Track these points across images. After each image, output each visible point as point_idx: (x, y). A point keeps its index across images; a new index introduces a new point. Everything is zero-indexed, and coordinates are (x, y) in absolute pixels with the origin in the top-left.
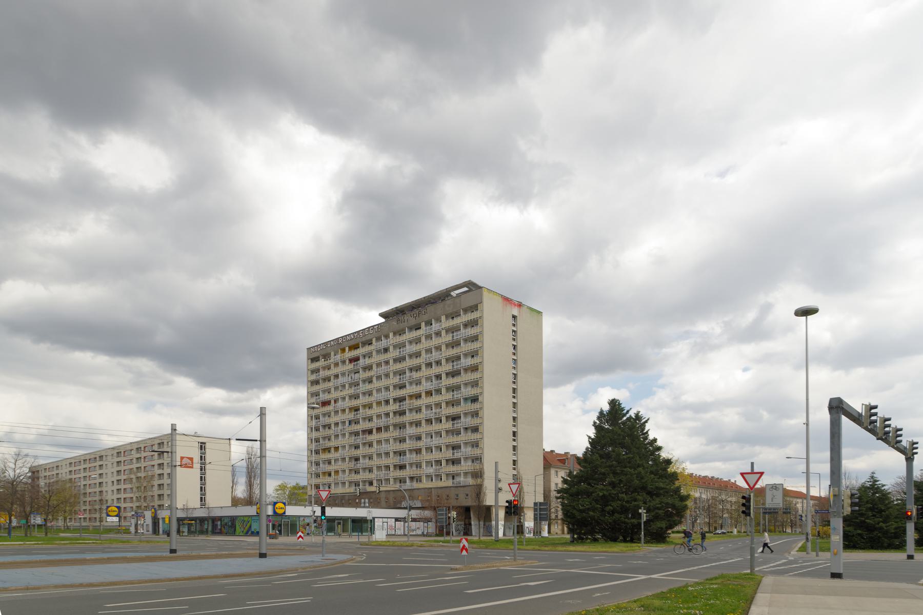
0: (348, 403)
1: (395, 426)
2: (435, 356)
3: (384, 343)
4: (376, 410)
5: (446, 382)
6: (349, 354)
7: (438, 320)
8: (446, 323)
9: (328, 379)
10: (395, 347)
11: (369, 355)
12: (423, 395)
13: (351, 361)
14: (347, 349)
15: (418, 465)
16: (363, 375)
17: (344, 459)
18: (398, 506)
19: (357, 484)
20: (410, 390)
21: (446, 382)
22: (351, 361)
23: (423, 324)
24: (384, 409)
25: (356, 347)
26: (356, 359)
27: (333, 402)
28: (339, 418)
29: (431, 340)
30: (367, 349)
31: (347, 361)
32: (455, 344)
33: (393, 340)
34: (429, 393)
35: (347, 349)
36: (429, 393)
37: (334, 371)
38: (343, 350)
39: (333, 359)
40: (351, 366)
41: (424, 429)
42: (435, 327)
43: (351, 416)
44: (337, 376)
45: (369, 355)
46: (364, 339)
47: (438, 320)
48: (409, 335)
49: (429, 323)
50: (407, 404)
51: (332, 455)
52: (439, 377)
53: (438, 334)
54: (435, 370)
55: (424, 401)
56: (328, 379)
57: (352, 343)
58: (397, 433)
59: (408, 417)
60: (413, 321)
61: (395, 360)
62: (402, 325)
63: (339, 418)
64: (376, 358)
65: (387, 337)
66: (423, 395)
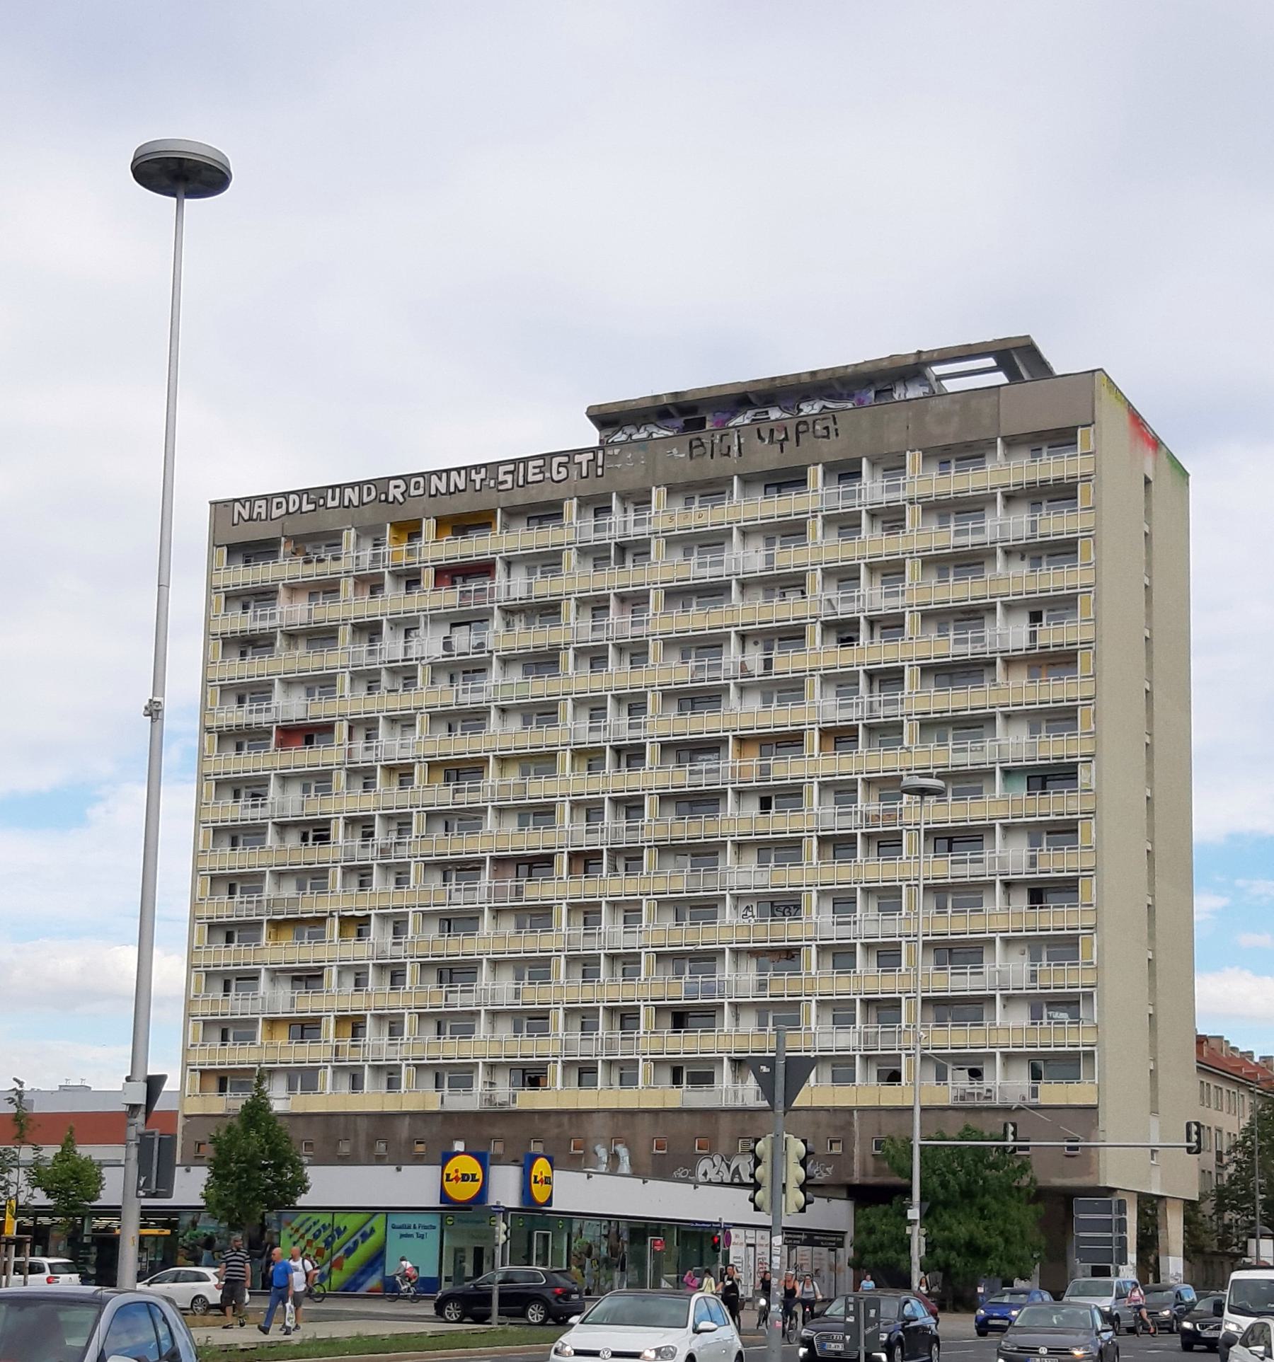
0: (424, 743)
1: (668, 850)
2: (871, 597)
4: (568, 781)
5: (919, 699)
6: (435, 549)
7: (893, 465)
9: (322, 636)
10: (672, 542)
11: (549, 561)
12: (813, 740)
13: (448, 574)
14: (429, 526)
15: (785, 1013)
16: (497, 637)
17: (396, 974)
19: (461, 1075)
20: (744, 713)
21: (919, 699)
22: (448, 574)
23: (816, 474)
24: (613, 780)
26: (484, 569)
27: (342, 730)
28: (383, 797)
29: (863, 538)
30: (523, 538)
31: (428, 576)
32: (969, 561)
33: (665, 514)
34: (840, 737)
35: (429, 526)
36: (840, 737)
37: (351, 606)
38: (410, 530)
39: (355, 554)
40: (449, 598)
41: (813, 871)
42: (872, 489)
43: (432, 793)
44: (369, 630)
45: (549, 561)
46: (520, 498)
47: (893, 465)
48: (745, 507)
49: (846, 472)
50: (733, 767)
51: (332, 950)
52: (888, 678)
53: (891, 518)
54: (871, 651)
55: (812, 764)
56: (322, 636)
57: (461, 505)
58: (678, 879)
59: (738, 819)
60: (767, 457)
61: (678, 595)
62: (712, 467)
63: (383, 797)
64: (576, 578)
65: (640, 500)
66: (813, 740)
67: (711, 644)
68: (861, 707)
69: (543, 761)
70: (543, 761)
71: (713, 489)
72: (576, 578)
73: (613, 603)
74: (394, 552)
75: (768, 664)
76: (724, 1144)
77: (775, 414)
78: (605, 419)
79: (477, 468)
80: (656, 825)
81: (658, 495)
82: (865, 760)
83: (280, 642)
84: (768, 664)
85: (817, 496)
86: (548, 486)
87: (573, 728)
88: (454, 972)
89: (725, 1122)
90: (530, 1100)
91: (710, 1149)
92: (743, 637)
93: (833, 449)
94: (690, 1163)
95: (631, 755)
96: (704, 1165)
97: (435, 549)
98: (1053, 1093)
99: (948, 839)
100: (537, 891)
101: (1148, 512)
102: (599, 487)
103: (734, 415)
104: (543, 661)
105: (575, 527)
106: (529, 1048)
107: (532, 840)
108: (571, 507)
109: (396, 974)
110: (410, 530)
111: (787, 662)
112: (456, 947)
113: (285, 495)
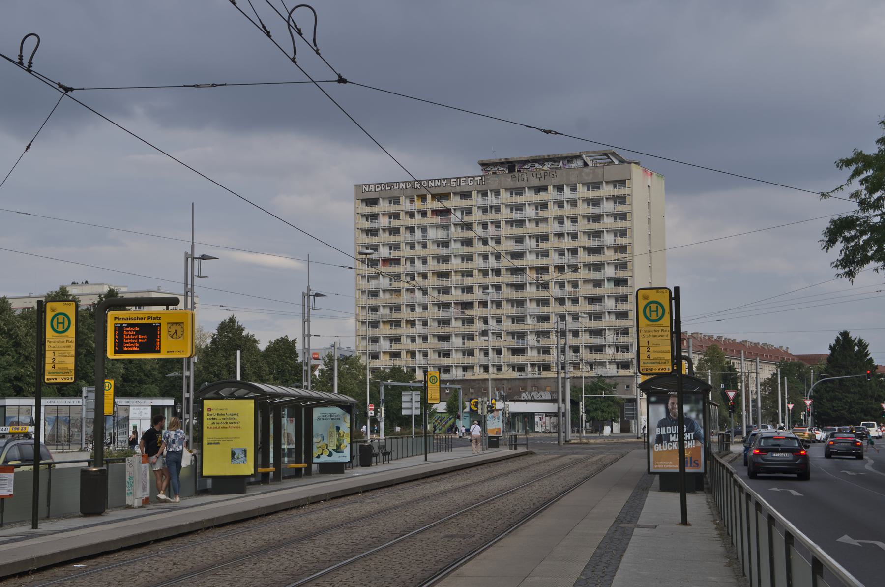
3: (491, 199)
8: (582, 192)
13: (437, 212)
14: (429, 197)
18: (516, 397)
22: (437, 212)
23: (550, 188)
24: (492, 279)
25: (445, 196)
31: (429, 213)
33: (505, 197)
35: (429, 197)
36: (560, 268)
38: (423, 198)
39: (405, 205)
40: (437, 220)
42: (567, 193)
46: (458, 190)
51: (404, 330)
54: (567, 242)
60: (536, 182)
62: (519, 184)
65: (497, 194)
67: (519, 240)
68: (568, 259)
69: (469, 274)
70: (469, 274)
71: (519, 192)
72: (478, 216)
73: (489, 224)
74: (418, 205)
75: (538, 245)
76: (529, 388)
77: (537, 165)
78: (485, 165)
79: (444, 179)
80: (507, 293)
81: (502, 192)
82: (569, 275)
83: (381, 231)
84: (538, 245)
85: (551, 195)
86: (467, 187)
87: (478, 263)
88: (445, 338)
89: (529, 383)
90: (469, 376)
91: (524, 389)
92: (530, 236)
93: (556, 181)
94: (520, 394)
95: (497, 272)
96: (523, 395)
97: (432, 204)
98: (623, 372)
99: (593, 300)
100: (469, 313)
101: (650, 196)
102: (484, 188)
103: (524, 165)
104: (468, 242)
105: (477, 200)
106: (468, 361)
107: (467, 297)
108: (474, 194)
109: (425, 338)
110: (423, 198)
111: (543, 246)
112: (445, 330)
113: (380, 184)
